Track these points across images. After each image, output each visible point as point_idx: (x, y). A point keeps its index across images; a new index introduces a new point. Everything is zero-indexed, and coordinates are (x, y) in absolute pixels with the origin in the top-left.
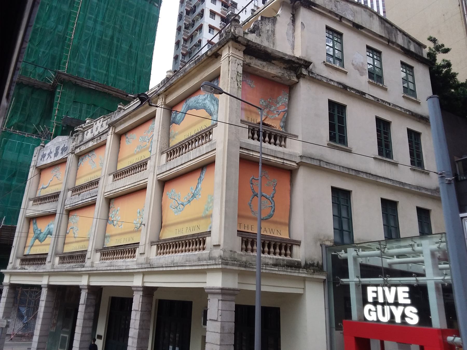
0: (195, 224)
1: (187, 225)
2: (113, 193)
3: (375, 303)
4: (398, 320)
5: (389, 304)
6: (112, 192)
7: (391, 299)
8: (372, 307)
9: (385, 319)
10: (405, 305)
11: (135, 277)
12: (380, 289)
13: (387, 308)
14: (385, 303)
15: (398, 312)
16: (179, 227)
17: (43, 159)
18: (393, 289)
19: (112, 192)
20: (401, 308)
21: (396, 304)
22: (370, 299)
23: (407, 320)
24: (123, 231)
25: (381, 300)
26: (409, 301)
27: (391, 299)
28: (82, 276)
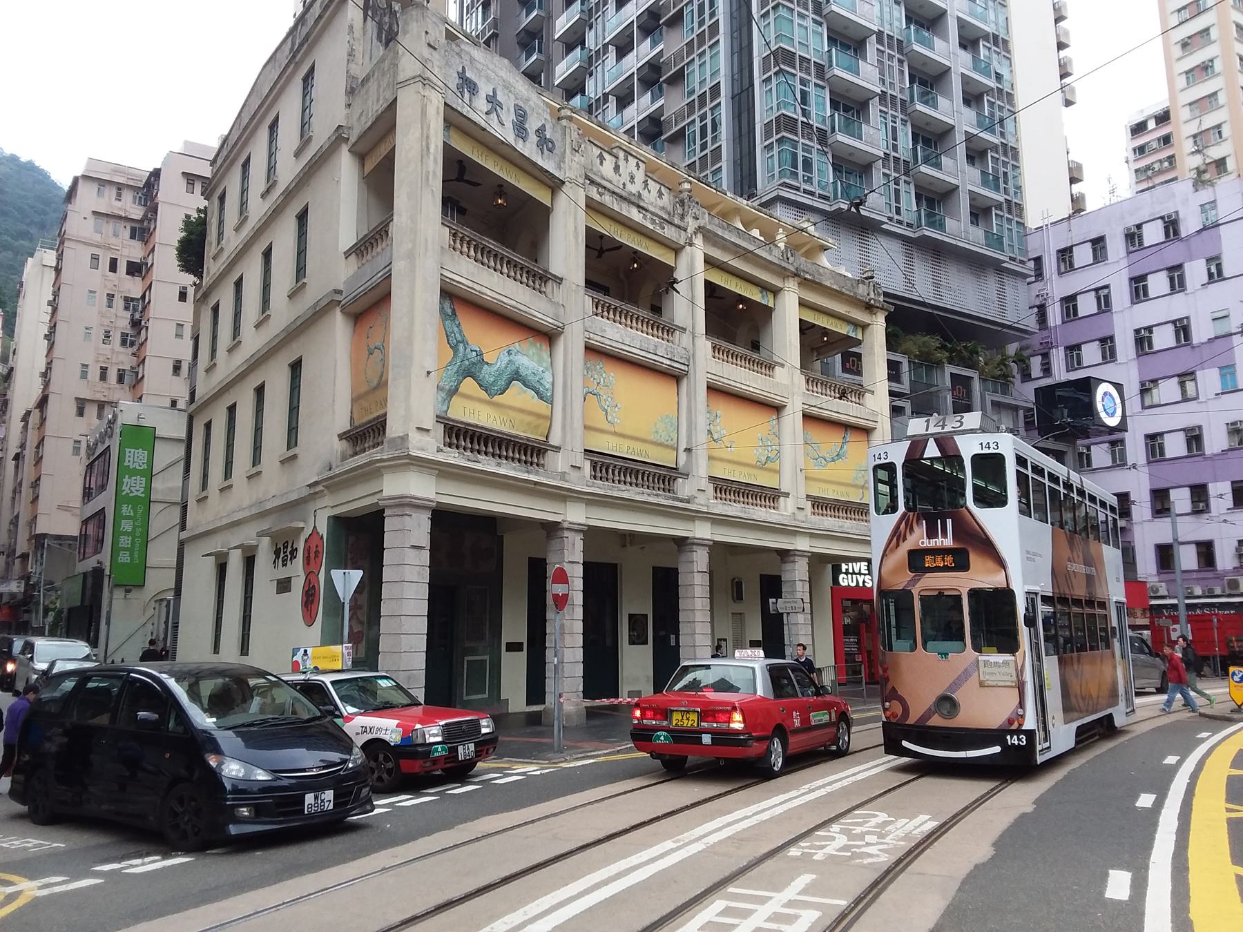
0: (843, 489)
1: (836, 487)
2: (723, 383)
3: (847, 573)
4: (861, 585)
5: (856, 574)
6: (722, 380)
7: (857, 571)
8: (845, 576)
9: (854, 584)
10: (865, 575)
11: (798, 538)
12: (850, 564)
13: (854, 576)
14: (853, 573)
15: (861, 579)
16: (823, 485)
17: (467, 95)
18: (858, 563)
19: (722, 380)
20: (863, 576)
21: (860, 574)
22: (844, 570)
23: (866, 584)
24: (736, 459)
25: (851, 571)
26: (867, 572)
27: (857, 571)
28: (694, 521)
